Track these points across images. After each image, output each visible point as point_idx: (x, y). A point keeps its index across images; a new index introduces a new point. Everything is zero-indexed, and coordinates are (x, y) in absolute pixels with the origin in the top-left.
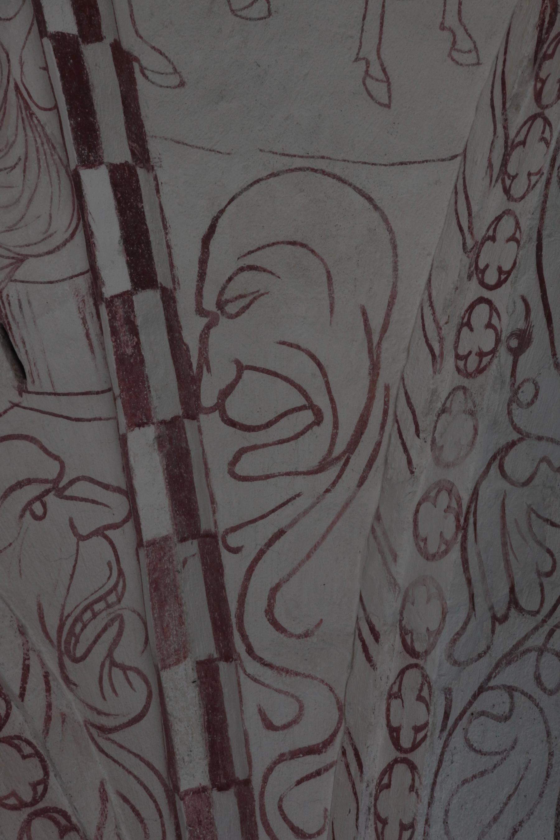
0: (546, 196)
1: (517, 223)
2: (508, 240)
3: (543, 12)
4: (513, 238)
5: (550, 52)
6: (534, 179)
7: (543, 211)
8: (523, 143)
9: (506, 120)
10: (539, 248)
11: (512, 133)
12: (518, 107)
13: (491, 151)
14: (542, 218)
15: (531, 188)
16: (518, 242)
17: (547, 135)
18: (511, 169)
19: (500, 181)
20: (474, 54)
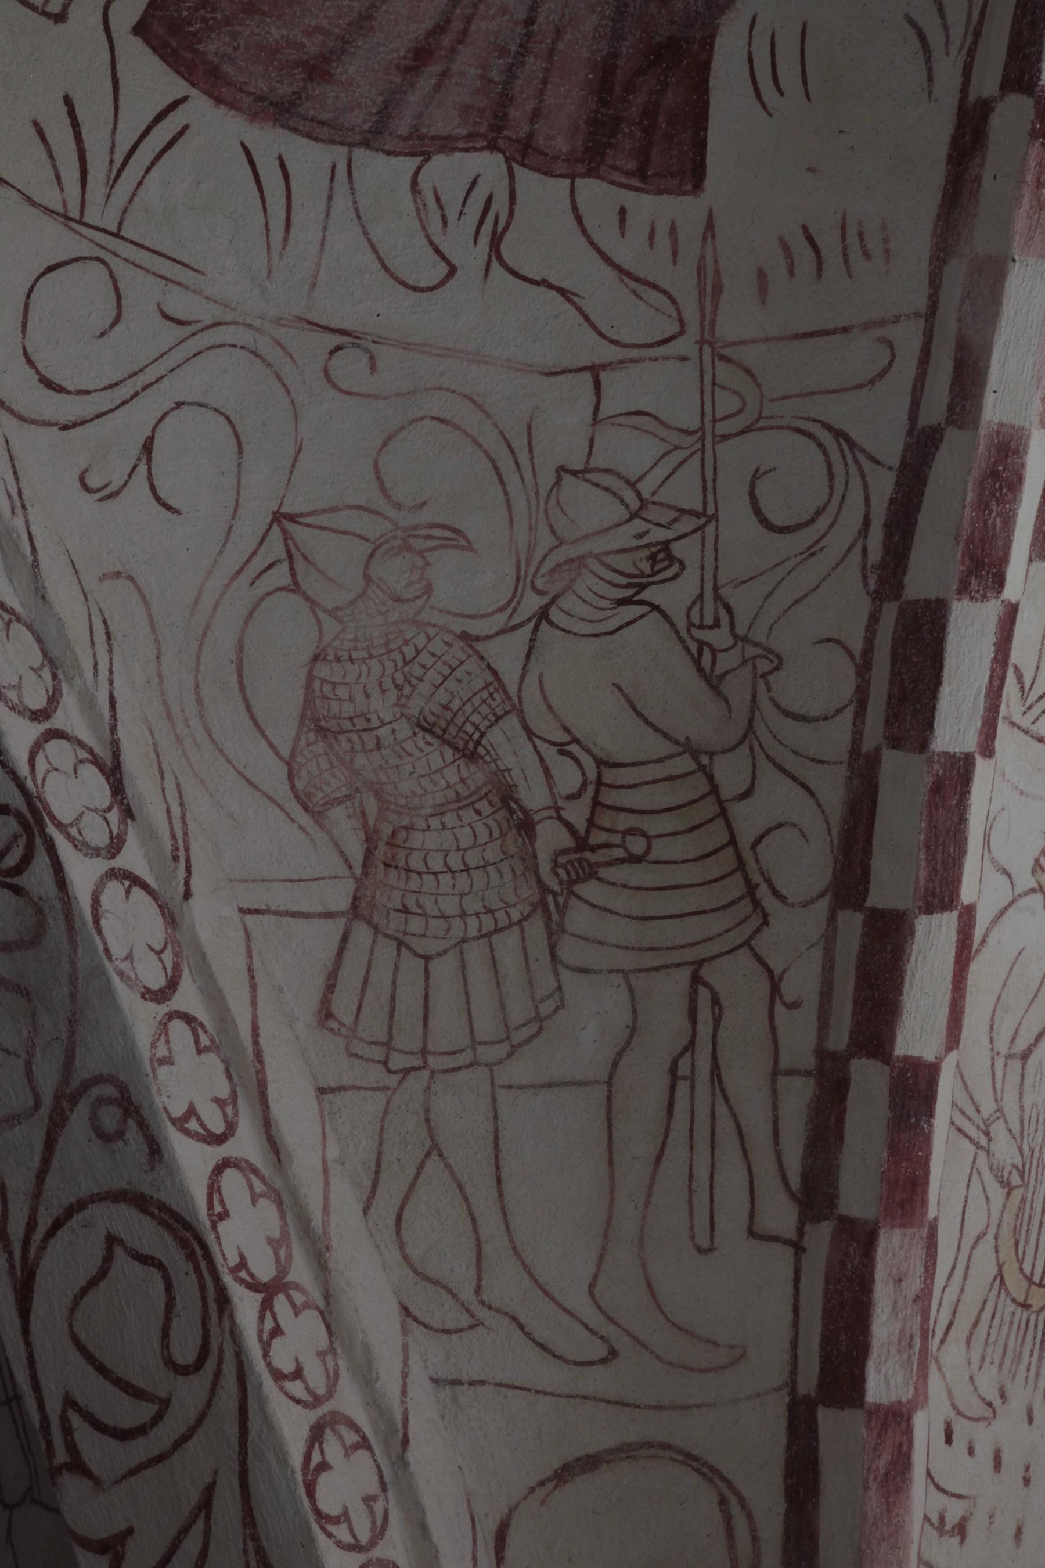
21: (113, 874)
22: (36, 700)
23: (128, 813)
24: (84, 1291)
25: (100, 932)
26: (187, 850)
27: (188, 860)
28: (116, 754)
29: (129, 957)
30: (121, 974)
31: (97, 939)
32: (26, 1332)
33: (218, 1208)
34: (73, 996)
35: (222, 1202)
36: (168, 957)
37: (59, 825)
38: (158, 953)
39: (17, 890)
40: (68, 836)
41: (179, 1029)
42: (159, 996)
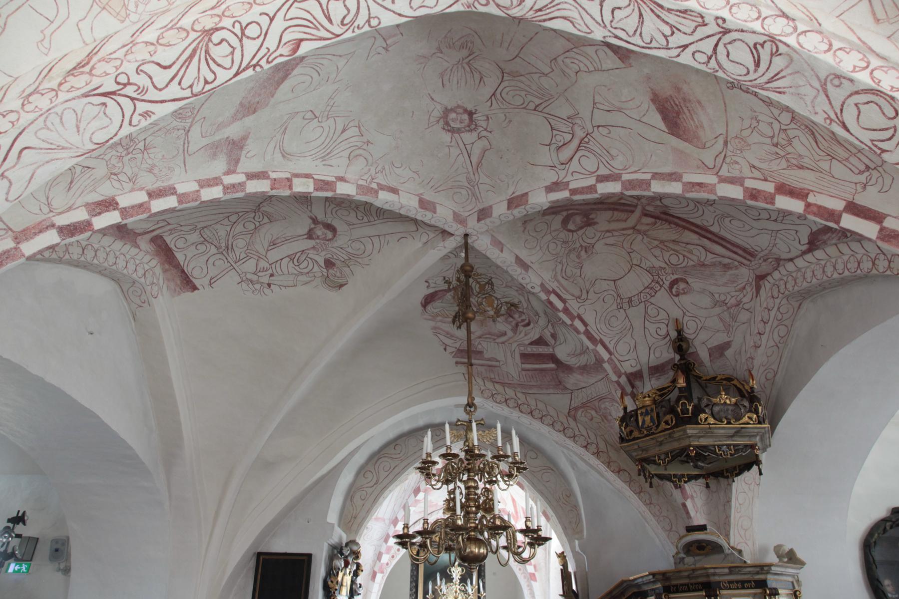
0: (37, 119)
1: (18, 119)
2: (10, 122)
3: (83, 61)
4: (12, 123)
5: (76, 74)
6: (37, 110)
7: (32, 123)
8: (43, 95)
9: (42, 82)
10: (20, 134)
11: (41, 88)
12: (50, 81)
13: (28, 87)
14: (30, 125)
15: (33, 111)
16: (13, 125)
17: (54, 99)
18: (31, 99)
19: (23, 99)
20: (47, 50)
21: (799, 35)
22: (756, 15)
23: (793, 20)
24: (858, 118)
25: (804, 48)
26: (813, 16)
27: (815, 18)
28: (782, 11)
29: (815, 48)
30: (816, 53)
31: (805, 50)
32: (851, 134)
33: (877, 81)
34: (809, 65)
35: (877, 79)
36: (825, 40)
37: (779, 35)
38: (822, 41)
39: (780, 54)
40: (782, 36)
41: (839, 53)
42: (829, 50)
